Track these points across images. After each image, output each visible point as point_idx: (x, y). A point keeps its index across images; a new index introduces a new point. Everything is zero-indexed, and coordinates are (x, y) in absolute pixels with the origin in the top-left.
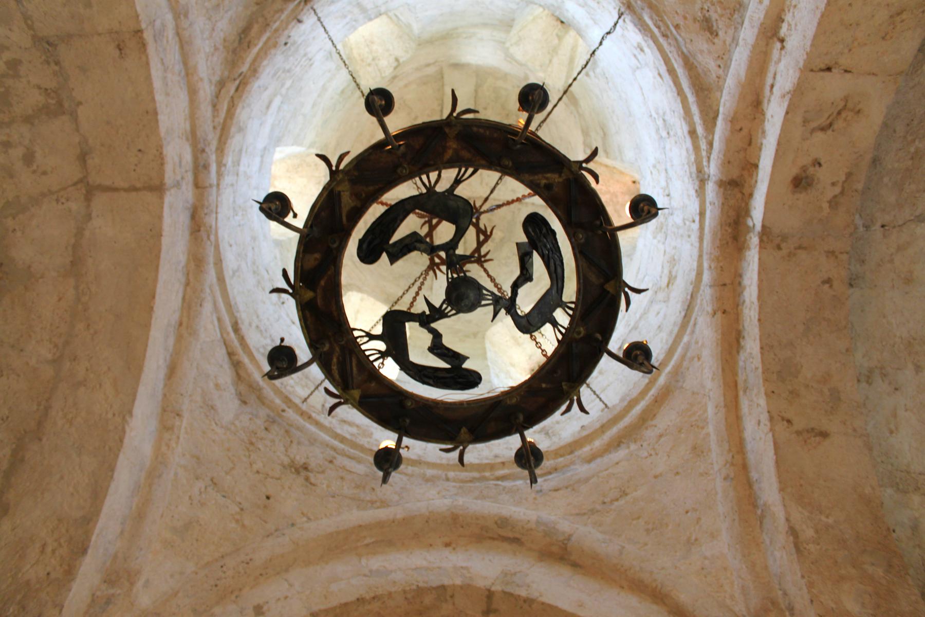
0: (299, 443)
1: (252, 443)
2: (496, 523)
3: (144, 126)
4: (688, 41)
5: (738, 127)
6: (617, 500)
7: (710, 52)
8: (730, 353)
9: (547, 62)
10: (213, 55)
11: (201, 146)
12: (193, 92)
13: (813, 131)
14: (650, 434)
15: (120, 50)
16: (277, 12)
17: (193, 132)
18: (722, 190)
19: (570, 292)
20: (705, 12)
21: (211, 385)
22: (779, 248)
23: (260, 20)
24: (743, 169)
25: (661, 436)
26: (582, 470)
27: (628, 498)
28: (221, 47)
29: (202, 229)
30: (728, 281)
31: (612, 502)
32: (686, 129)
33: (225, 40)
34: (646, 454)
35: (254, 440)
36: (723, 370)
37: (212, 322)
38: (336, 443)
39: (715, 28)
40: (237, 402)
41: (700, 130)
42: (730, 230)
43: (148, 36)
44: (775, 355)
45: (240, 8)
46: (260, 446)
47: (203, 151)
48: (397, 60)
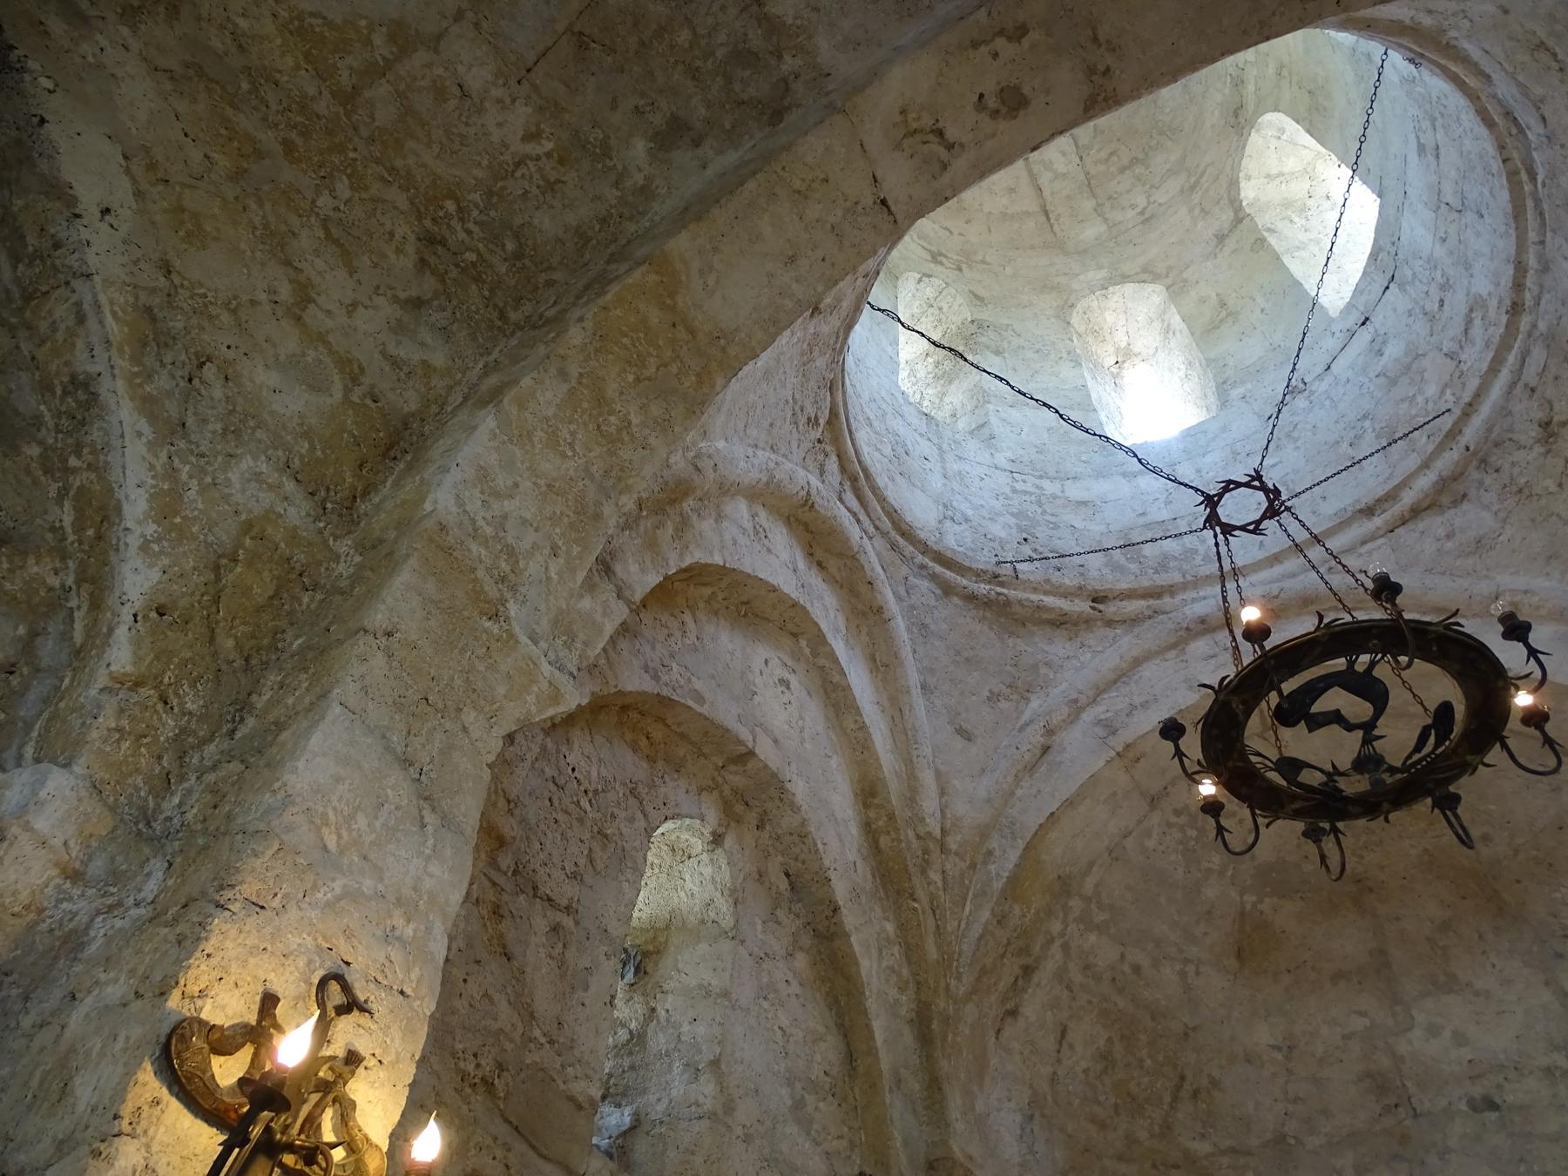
0: (1511, 430)
1: (1520, 491)
6: (1555, 55)
11: (1182, 633)
13: (950, 147)
14: (1427, 21)
17: (1174, 646)
19: (1340, 663)
21: (1449, 545)
22: (1107, 71)
35: (1515, 489)
37: (1370, 553)
38: (1504, 376)
40: (1465, 506)
44: (1274, 14)
46: (1523, 481)
47: (1188, 629)
48: (920, 281)
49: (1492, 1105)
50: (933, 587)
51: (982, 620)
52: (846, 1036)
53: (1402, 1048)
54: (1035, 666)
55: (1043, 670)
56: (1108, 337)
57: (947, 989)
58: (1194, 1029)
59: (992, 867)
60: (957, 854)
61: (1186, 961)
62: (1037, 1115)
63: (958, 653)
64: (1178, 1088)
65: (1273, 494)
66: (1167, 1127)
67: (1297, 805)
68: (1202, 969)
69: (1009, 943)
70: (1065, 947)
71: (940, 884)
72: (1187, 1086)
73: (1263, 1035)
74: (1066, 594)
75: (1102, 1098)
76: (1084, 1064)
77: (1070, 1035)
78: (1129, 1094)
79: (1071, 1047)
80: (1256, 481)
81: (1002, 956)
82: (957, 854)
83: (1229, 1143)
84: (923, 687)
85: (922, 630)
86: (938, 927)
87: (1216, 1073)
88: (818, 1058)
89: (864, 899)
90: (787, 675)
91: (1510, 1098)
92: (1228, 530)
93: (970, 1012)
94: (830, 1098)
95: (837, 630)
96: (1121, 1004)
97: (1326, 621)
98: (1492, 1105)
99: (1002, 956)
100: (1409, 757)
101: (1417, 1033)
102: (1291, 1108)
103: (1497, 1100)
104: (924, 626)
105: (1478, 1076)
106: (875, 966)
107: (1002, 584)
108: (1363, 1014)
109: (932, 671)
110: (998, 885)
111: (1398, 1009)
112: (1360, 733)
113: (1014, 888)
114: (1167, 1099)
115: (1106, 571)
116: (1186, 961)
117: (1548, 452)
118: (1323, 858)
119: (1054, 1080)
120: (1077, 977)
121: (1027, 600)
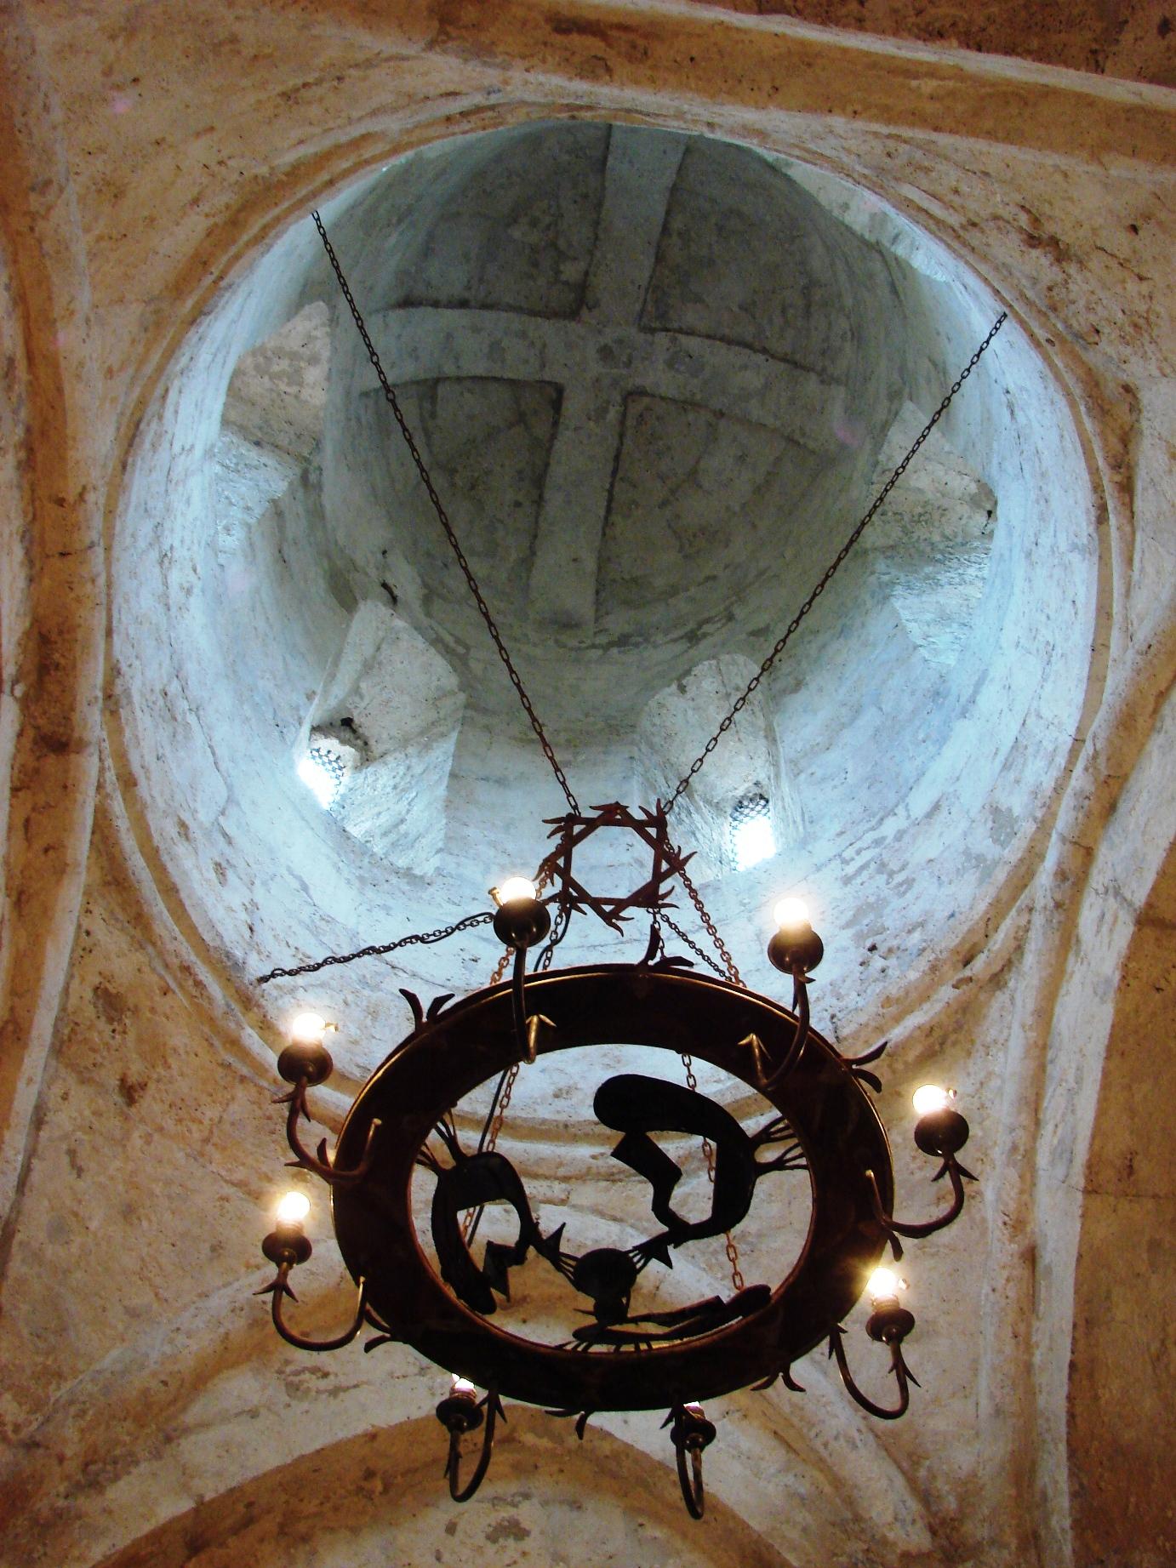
1: (1136, 326)
2: (609, 70)
3: (1136, 1032)
4: (146, 969)
5: (51, 853)
7: (107, 958)
8: (46, 420)
9: (384, 646)
10: (995, 1042)
12: (1045, 1015)
14: (222, 200)
15: (1131, 1167)
18: (76, 735)
20: (119, 1028)
24: (37, 771)
25: (196, 202)
26: (392, 124)
27: (280, 88)
28: (978, 1045)
29: (1102, 778)
30: (57, 562)
31: (319, 82)
32: (143, 789)
33: (969, 1054)
34: (231, 163)
35: (1130, 330)
36: (60, 390)
37: (1142, 570)
39: (100, 1003)
41: (118, 806)
42: (56, 656)
43: (1079, 1180)
47: (1058, 905)
48: (682, 689)
56: (945, 503)
60: (993, 1542)
74: (924, 994)
82: (993, 1542)
112: (532, 1251)
117: (1080, 262)
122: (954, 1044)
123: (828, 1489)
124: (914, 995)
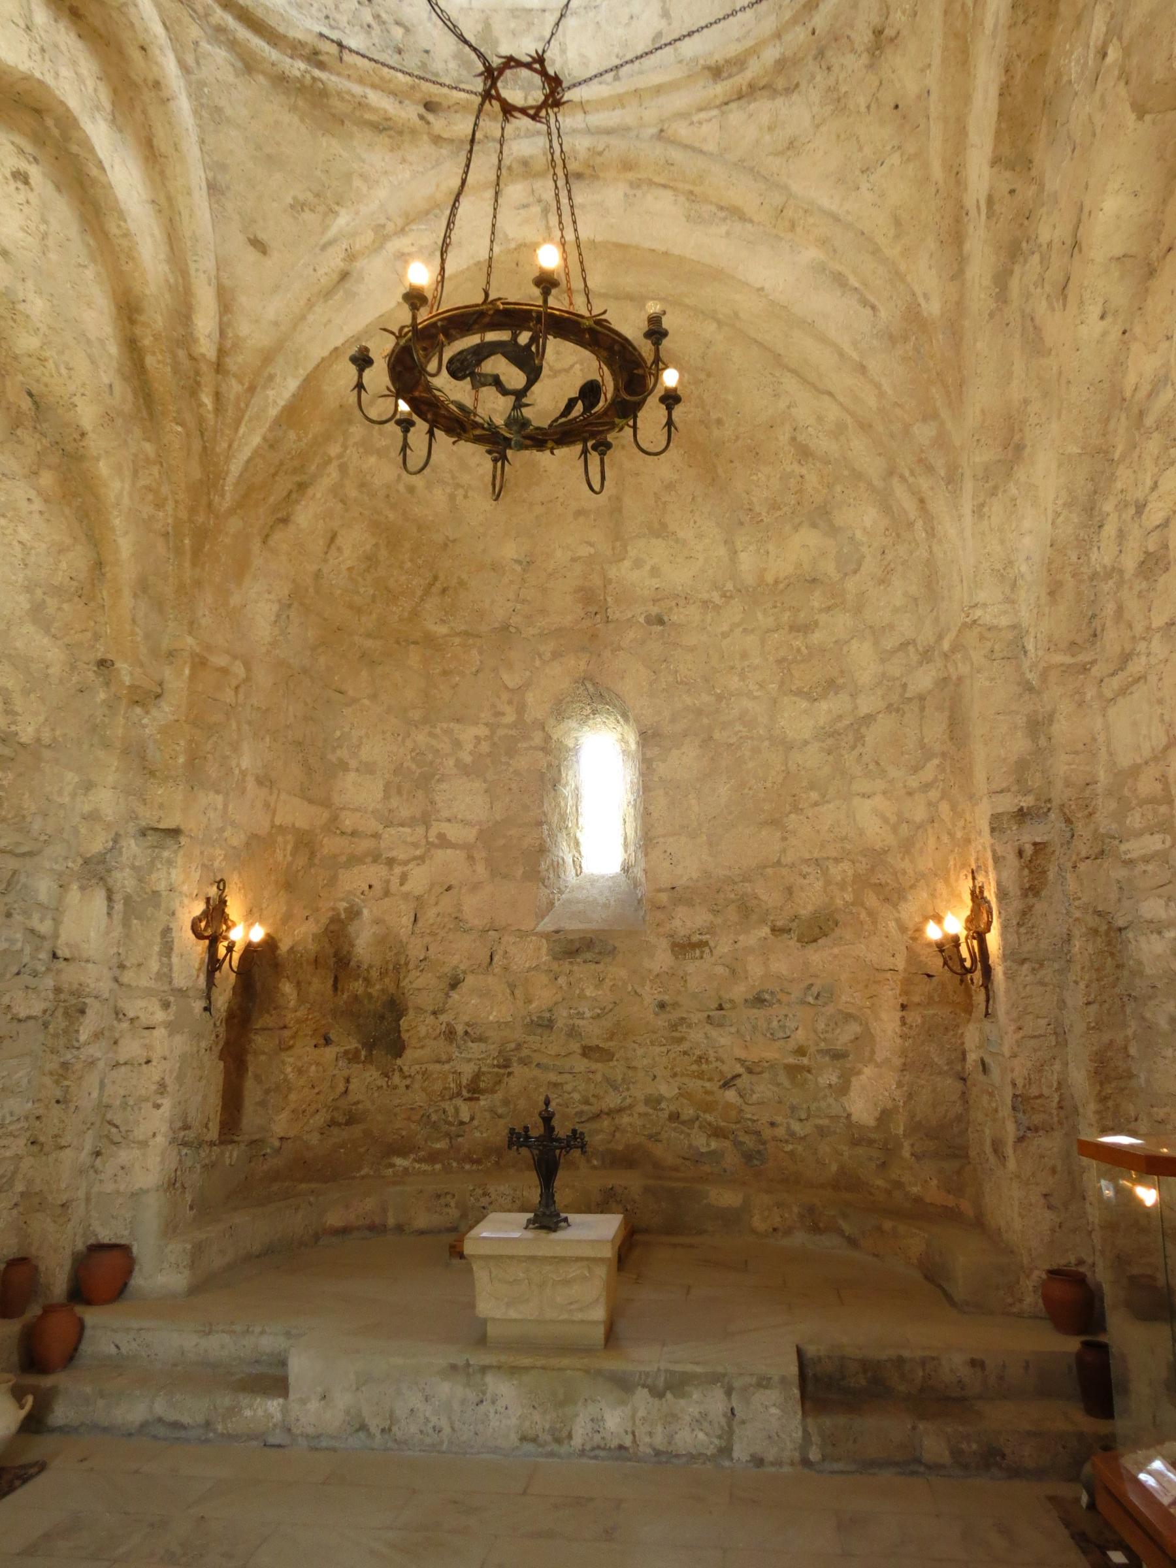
16: (342, 99)
19: (503, 336)
23: (358, 114)
33: (392, 150)
40: (795, 97)
45: (355, 143)
49: (660, 621)
50: (232, 58)
51: (293, 109)
52: (96, 546)
53: (613, 573)
54: (348, 176)
55: (357, 182)
57: (210, 505)
58: (454, 541)
59: (271, 393)
61: (458, 486)
62: (296, 605)
63: (259, 148)
64: (431, 585)
65: (554, 83)
66: (415, 613)
67: (478, 432)
68: (470, 494)
69: (282, 464)
70: (343, 469)
71: (210, 407)
72: (438, 585)
73: (510, 551)
75: (362, 590)
76: (349, 563)
77: (339, 541)
78: (386, 588)
79: (339, 549)
80: (538, 62)
81: (274, 475)
83: (463, 628)
84: (213, 188)
85: (211, 114)
86: (205, 448)
87: (464, 576)
88: (64, 565)
89: (119, 422)
90: (23, 165)
91: (674, 618)
92: (508, 110)
93: (234, 524)
94: (76, 599)
95: (98, 108)
96: (392, 516)
97: (490, 298)
98: (660, 621)
99: (274, 475)
100: (556, 420)
101: (627, 564)
102: (519, 606)
103: (666, 618)
104: (218, 110)
105: (658, 600)
106: (127, 486)
107: (321, 65)
108: (591, 544)
109: (223, 167)
110: (273, 412)
111: (618, 544)
113: (292, 414)
114: (419, 593)
115: (452, 65)
116: (458, 486)
118: (494, 477)
119: (318, 575)
120: (353, 493)
121: (349, 92)
122: (390, 137)
123: (181, 289)
124: (392, 86)
